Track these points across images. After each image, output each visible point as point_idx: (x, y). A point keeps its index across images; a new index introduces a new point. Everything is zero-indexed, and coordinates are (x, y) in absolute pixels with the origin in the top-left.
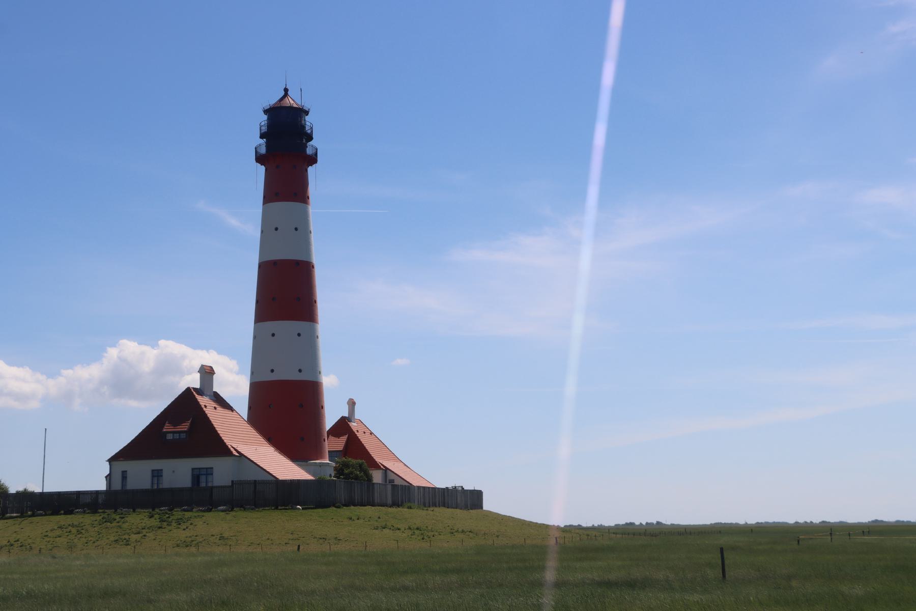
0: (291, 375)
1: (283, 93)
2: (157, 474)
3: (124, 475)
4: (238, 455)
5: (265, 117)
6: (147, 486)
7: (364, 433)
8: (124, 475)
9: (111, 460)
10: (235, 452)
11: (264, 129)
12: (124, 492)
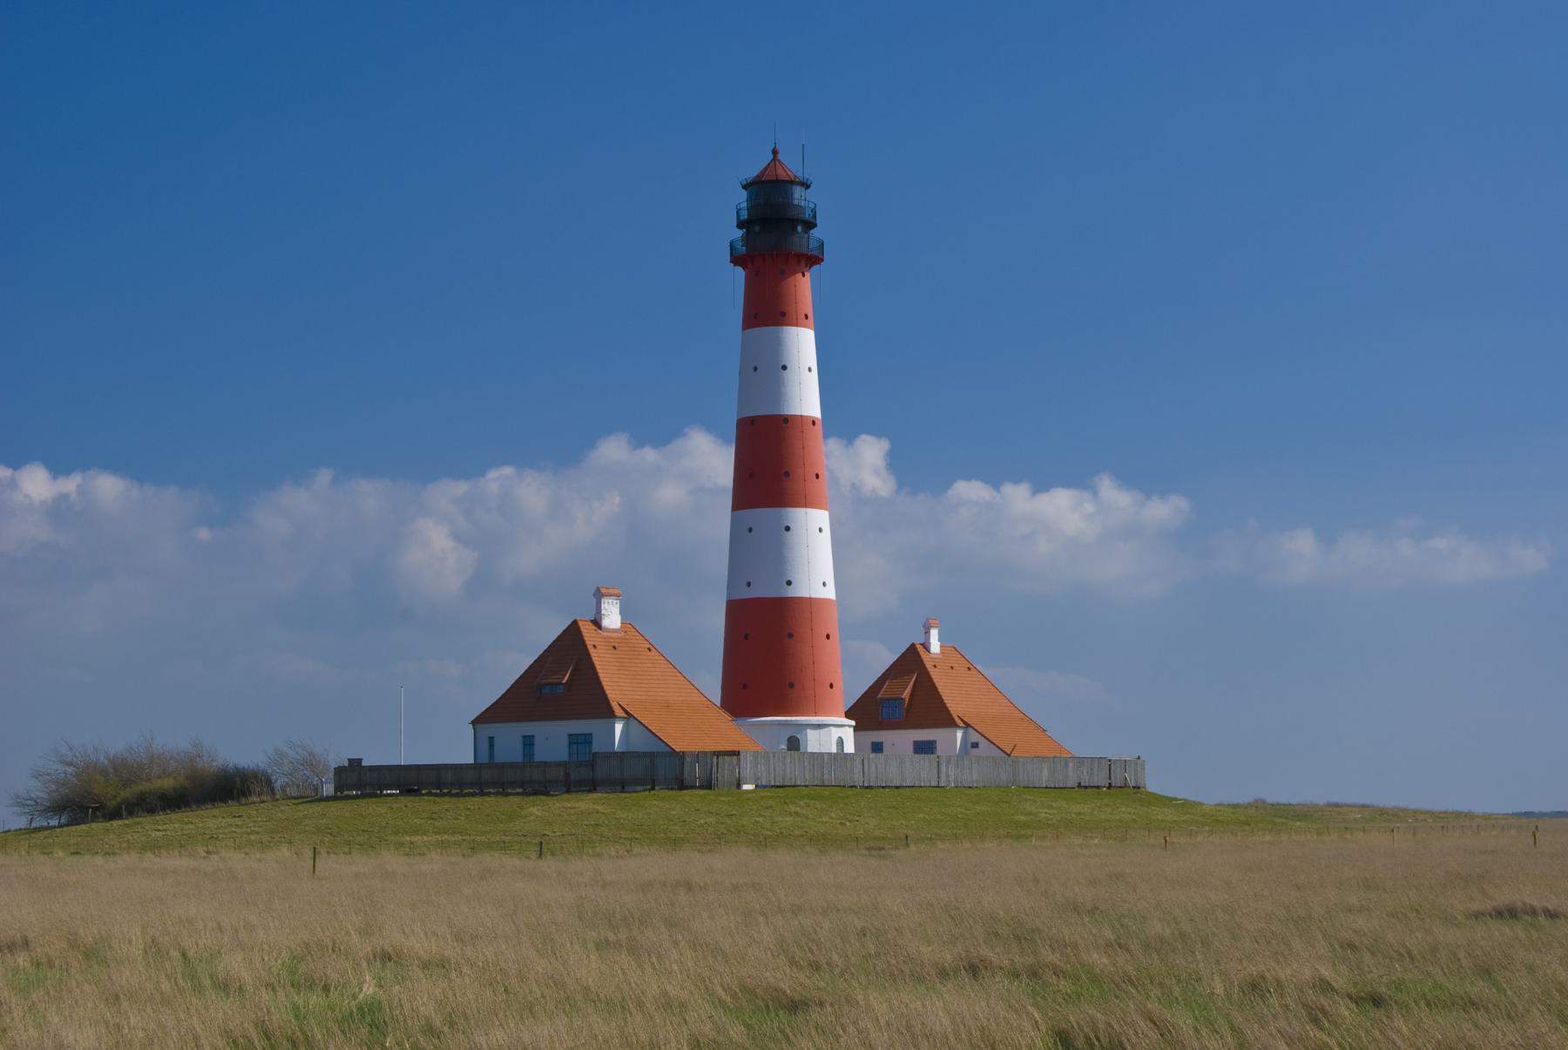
0: (760, 591)
1: (771, 157)
2: (528, 742)
3: (491, 739)
4: (625, 716)
5: (744, 194)
6: (520, 759)
7: (952, 668)
8: (491, 739)
9: (474, 722)
10: (622, 711)
11: (745, 215)
12: (492, 765)
